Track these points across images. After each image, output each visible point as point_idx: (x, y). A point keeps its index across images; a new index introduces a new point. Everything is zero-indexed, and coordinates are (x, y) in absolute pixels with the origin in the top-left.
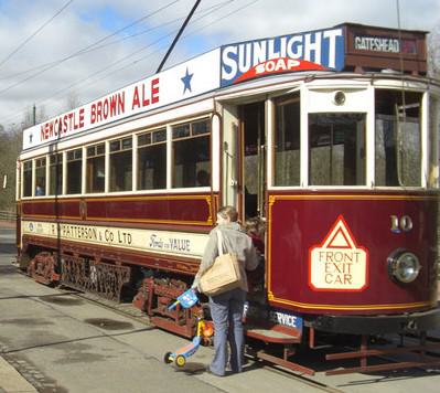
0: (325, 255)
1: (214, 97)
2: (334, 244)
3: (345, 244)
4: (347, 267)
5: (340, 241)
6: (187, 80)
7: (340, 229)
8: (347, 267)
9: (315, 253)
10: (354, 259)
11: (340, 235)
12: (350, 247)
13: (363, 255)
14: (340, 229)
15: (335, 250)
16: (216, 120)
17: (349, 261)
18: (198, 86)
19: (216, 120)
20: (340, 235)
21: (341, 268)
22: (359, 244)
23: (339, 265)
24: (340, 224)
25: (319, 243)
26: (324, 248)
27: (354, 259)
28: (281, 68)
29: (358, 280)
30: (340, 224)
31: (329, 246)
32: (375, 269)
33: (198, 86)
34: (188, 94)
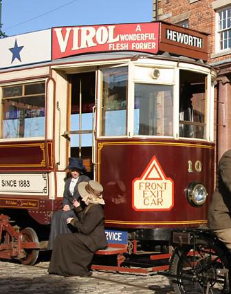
0: (144, 185)
1: (50, 65)
2: (149, 177)
3: (159, 177)
4: (160, 193)
5: (154, 174)
6: (16, 51)
7: (154, 165)
8: (160, 193)
9: (136, 183)
10: (163, 189)
11: (154, 170)
12: (161, 179)
13: (169, 183)
14: (154, 165)
15: (148, 181)
16: (51, 84)
17: (160, 189)
18: (26, 57)
19: (51, 83)
20: (154, 170)
21: (156, 194)
22: (168, 176)
23: (153, 192)
24: (154, 162)
25: (139, 176)
26: (143, 180)
27: (163, 189)
28: (106, 44)
29: (167, 203)
30: (154, 162)
31: (146, 179)
32: (180, 197)
33: (26, 57)
34: (16, 62)
